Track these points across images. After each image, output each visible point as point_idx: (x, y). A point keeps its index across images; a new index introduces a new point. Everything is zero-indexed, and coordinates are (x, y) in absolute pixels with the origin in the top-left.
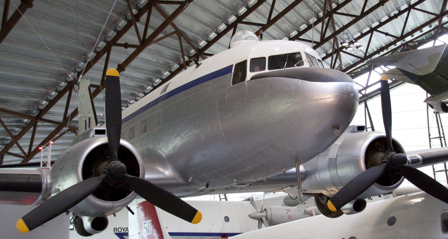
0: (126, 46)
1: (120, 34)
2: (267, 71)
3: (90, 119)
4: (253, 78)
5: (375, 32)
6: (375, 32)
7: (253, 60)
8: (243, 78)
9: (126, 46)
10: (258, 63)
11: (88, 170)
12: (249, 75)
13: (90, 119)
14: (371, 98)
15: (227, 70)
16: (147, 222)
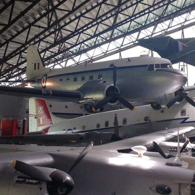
0: (39, 27)
1: (36, 20)
2: (160, 68)
3: (39, 63)
4: (157, 70)
5: (132, 22)
6: (132, 22)
7: (156, 65)
8: (153, 69)
9: (39, 27)
10: (157, 66)
11: (107, 94)
12: (155, 69)
13: (39, 63)
14: (123, 50)
15: (146, 66)
16: (41, 108)
